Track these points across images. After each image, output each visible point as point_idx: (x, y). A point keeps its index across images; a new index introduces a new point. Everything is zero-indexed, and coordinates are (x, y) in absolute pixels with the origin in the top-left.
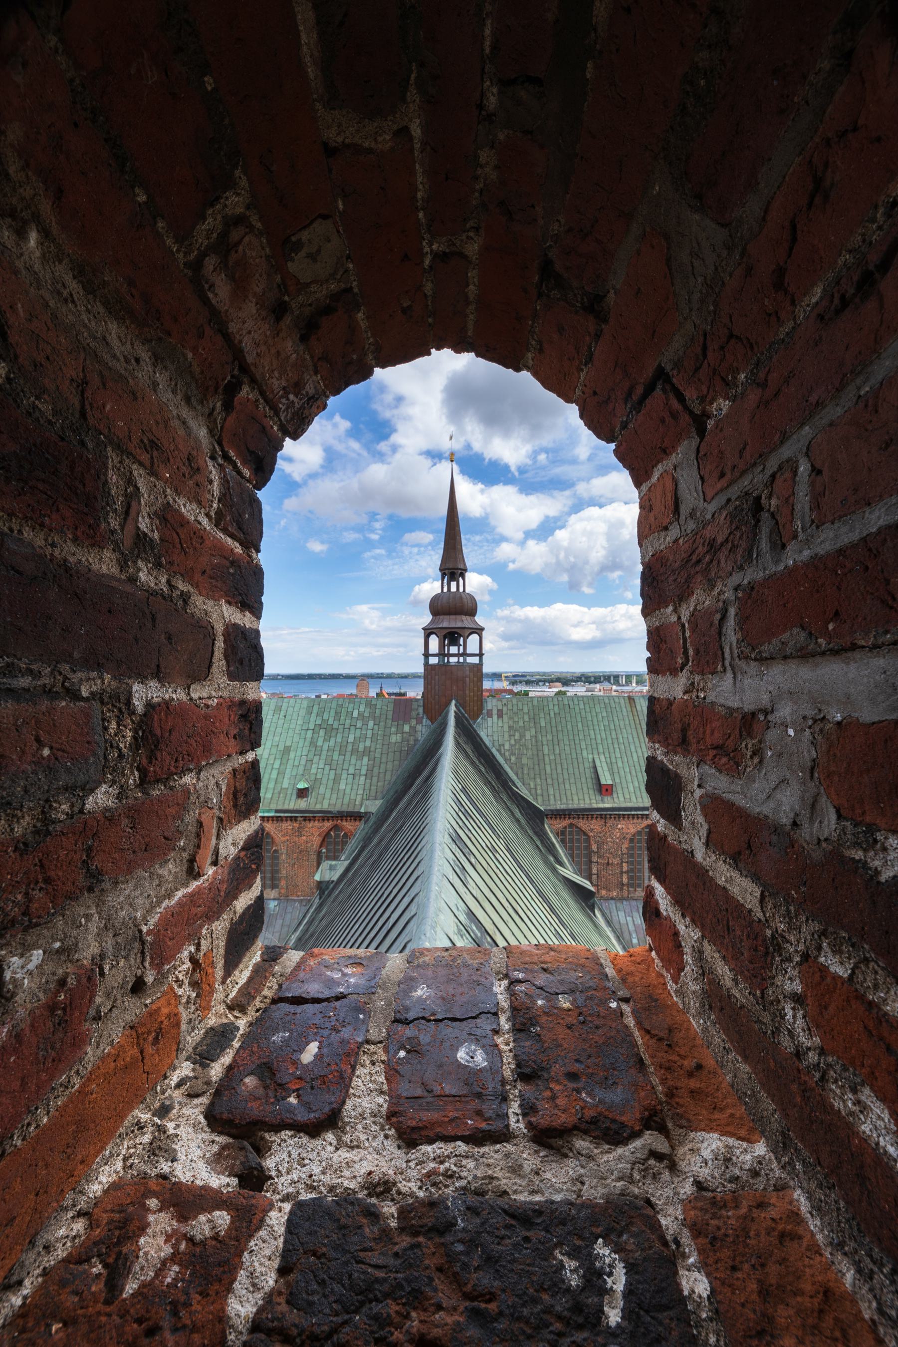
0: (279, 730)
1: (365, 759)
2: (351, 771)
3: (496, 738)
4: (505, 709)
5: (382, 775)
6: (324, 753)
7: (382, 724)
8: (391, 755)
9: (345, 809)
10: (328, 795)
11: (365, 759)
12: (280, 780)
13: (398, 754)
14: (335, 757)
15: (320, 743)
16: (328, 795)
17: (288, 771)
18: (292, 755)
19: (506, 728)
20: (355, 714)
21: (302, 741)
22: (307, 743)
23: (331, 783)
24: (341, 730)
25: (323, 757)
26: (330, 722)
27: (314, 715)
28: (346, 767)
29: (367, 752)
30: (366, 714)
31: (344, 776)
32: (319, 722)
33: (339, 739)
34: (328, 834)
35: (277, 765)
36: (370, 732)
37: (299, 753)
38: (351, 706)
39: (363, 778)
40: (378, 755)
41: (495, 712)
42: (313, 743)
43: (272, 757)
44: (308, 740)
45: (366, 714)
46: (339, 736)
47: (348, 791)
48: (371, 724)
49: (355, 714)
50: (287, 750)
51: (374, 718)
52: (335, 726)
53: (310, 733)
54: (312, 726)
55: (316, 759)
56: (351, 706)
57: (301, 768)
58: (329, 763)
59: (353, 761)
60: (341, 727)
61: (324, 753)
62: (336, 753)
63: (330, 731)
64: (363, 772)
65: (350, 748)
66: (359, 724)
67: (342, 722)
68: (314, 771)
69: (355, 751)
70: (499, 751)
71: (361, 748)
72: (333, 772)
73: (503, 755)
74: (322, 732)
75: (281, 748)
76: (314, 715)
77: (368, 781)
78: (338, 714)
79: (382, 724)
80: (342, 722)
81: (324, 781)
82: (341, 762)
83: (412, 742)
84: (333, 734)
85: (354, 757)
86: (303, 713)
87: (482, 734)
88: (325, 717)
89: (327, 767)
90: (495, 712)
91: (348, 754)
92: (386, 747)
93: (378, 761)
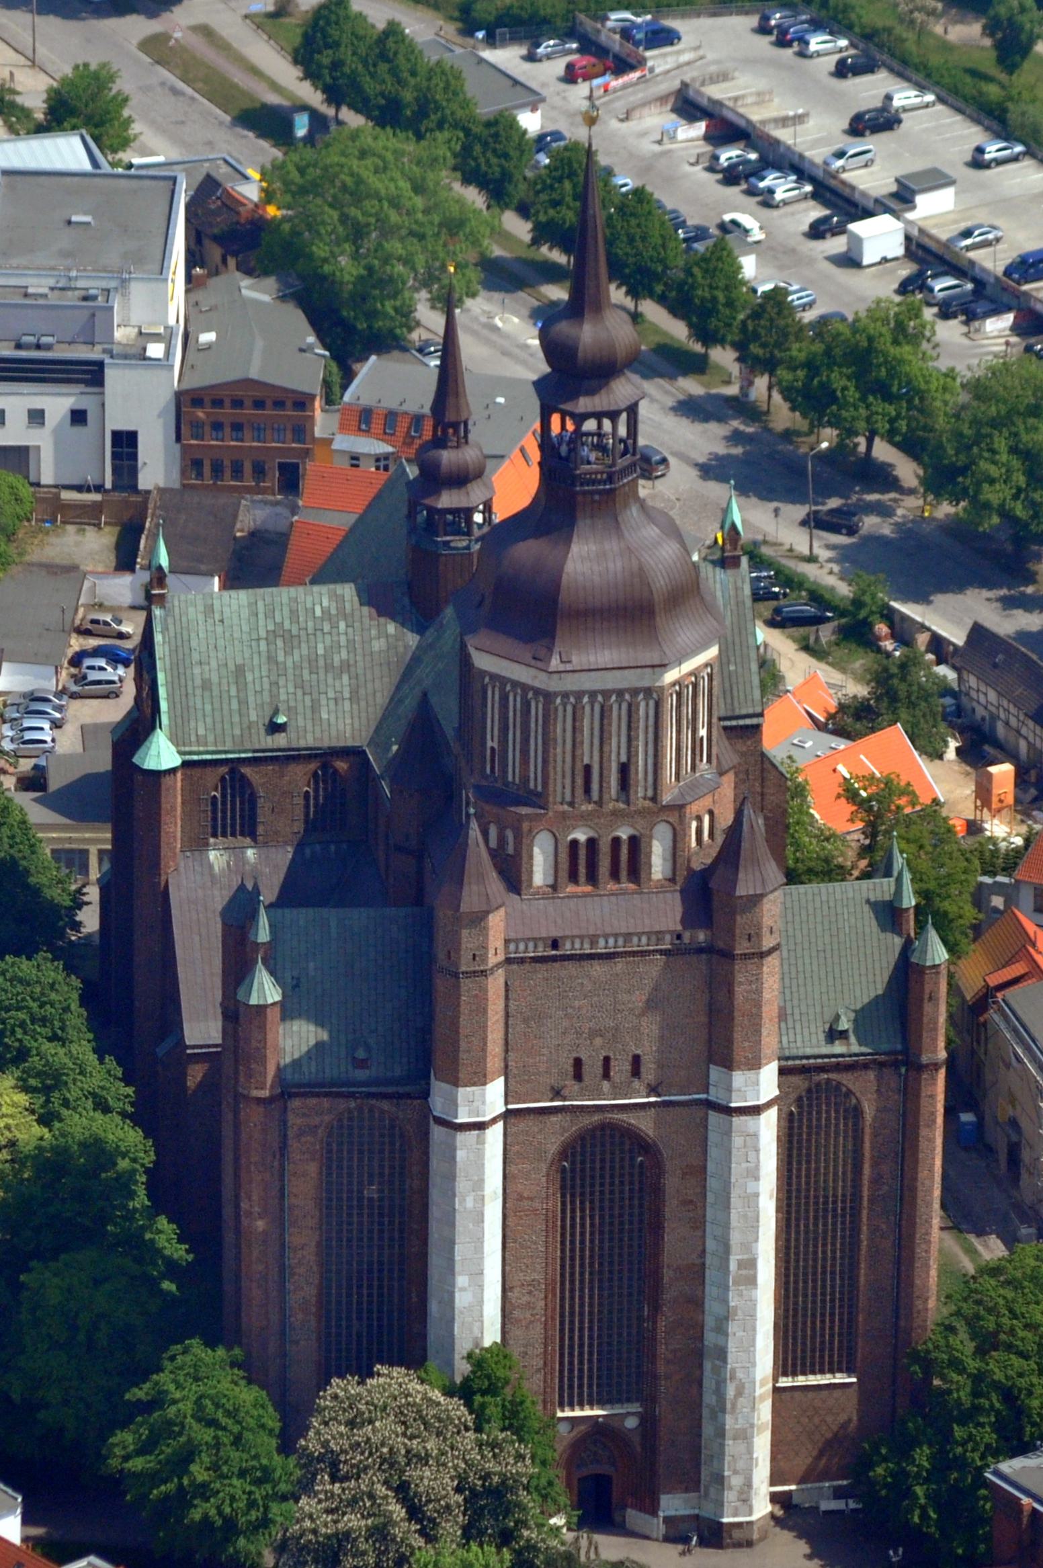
1: (345, 678)
2: (331, 694)
5: (370, 698)
6: (290, 671)
11: (345, 678)
14: (306, 676)
15: (281, 658)
17: (251, 699)
18: (249, 677)
21: (256, 657)
22: (264, 659)
24: (304, 638)
29: (346, 667)
32: (271, 627)
35: (233, 692)
39: (347, 704)
40: (360, 671)
42: (271, 659)
44: (264, 654)
52: (295, 632)
54: (263, 634)
57: (266, 694)
58: (300, 685)
59: (330, 681)
64: (347, 695)
65: (321, 662)
69: (328, 667)
71: (337, 663)
72: (308, 698)
74: (280, 643)
75: (232, 667)
80: (303, 625)
81: (300, 709)
84: (295, 643)
85: (330, 676)
89: (299, 692)
93: (362, 678)
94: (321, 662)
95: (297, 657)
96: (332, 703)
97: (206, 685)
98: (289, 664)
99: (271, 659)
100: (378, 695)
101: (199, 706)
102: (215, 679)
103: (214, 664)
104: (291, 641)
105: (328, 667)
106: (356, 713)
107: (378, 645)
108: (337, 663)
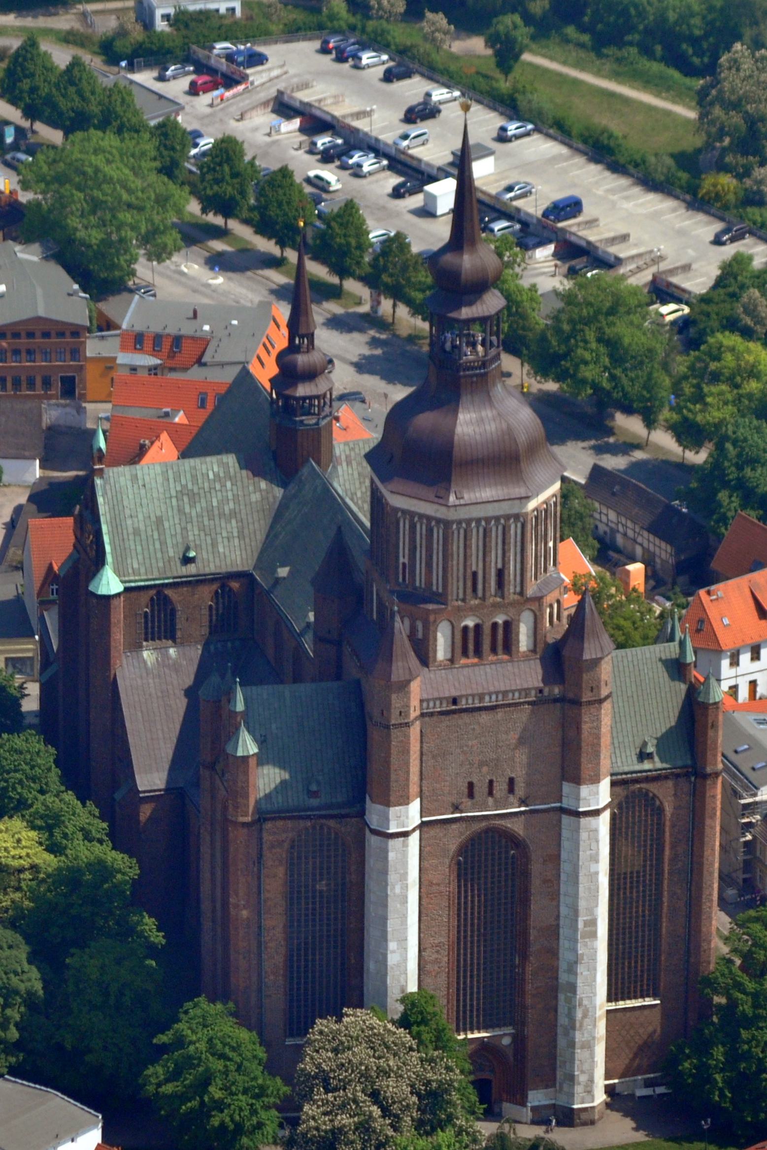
0: (144, 501)
1: (234, 522)
2: (225, 534)
3: (348, 486)
4: (353, 454)
5: (252, 536)
6: (195, 519)
7: (239, 484)
8: (255, 515)
9: (230, 569)
10: (211, 559)
11: (234, 522)
12: (164, 549)
13: (261, 513)
14: (206, 523)
15: (187, 510)
16: (211, 559)
18: (166, 525)
19: (356, 475)
20: (211, 476)
21: (170, 510)
22: (175, 511)
23: (210, 548)
24: (202, 495)
25: (195, 524)
26: (190, 486)
27: (171, 480)
28: (218, 530)
29: (233, 514)
30: (222, 475)
31: (220, 540)
32: (179, 488)
33: (204, 505)
34: (217, 592)
36: (230, 494)
37: (171, 522)
38: (204, 467)
39: (236, 541)
40: (244, 516)
41: (343, 457)
42: (181, 511)
43: (149, 529)
44: (175, 508)
45: (222, 475)
46: (203, 500)
47: (227, 553)
48: (229, 484)
49: (211, 476)
50: (159, 521)
51: (230, 479)
52: (196, 491)
53: (174, 501)
54: (174, 493)
55: (189, 526)
56: (204, 467)
58: (202, 528)
59: (223, 525)
60: (202, 491)
61: (195, 519)
62: (206, 519)
63: (193, 497)
64: (236, 534)
65: (216, 512)
66: (218, 487)
67: (201, 485)
68: (191, 538)
69: (222, 515)
70: (352, 499)
71: (227, 511)
73: (356, 504)
74: (186, 499)
75: (153, 519)
76: (171, 480)
77: (242, 542)
78: (194, 478)
79: (239, 484)
80: (201, 485)
81: (204, 546)
82: (212, 527)
83: (271, 500)
84: (197, 499)
86: (160, 479)
87: (336, 485)
88: (183, 482)
89: (202, 534)
90: (343, 457)
91: (217, 518)
92: (248, 507)
93: (245, 521)
94: (216, 512)
95: (199, 509)
96: (226, 541)
97: (137, 532)
98: (194, 514)
99: (181, 511)
100: (258, 533)
101: (133, 547)
102: (142, 527)
103: (140, 517)
104: (193, 497)
105: (222, 515)
106: (243, 546)
107: (255, 497)
108: (227, 511)
